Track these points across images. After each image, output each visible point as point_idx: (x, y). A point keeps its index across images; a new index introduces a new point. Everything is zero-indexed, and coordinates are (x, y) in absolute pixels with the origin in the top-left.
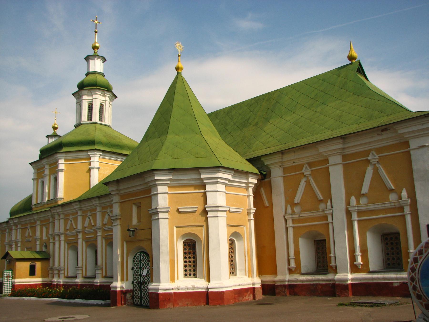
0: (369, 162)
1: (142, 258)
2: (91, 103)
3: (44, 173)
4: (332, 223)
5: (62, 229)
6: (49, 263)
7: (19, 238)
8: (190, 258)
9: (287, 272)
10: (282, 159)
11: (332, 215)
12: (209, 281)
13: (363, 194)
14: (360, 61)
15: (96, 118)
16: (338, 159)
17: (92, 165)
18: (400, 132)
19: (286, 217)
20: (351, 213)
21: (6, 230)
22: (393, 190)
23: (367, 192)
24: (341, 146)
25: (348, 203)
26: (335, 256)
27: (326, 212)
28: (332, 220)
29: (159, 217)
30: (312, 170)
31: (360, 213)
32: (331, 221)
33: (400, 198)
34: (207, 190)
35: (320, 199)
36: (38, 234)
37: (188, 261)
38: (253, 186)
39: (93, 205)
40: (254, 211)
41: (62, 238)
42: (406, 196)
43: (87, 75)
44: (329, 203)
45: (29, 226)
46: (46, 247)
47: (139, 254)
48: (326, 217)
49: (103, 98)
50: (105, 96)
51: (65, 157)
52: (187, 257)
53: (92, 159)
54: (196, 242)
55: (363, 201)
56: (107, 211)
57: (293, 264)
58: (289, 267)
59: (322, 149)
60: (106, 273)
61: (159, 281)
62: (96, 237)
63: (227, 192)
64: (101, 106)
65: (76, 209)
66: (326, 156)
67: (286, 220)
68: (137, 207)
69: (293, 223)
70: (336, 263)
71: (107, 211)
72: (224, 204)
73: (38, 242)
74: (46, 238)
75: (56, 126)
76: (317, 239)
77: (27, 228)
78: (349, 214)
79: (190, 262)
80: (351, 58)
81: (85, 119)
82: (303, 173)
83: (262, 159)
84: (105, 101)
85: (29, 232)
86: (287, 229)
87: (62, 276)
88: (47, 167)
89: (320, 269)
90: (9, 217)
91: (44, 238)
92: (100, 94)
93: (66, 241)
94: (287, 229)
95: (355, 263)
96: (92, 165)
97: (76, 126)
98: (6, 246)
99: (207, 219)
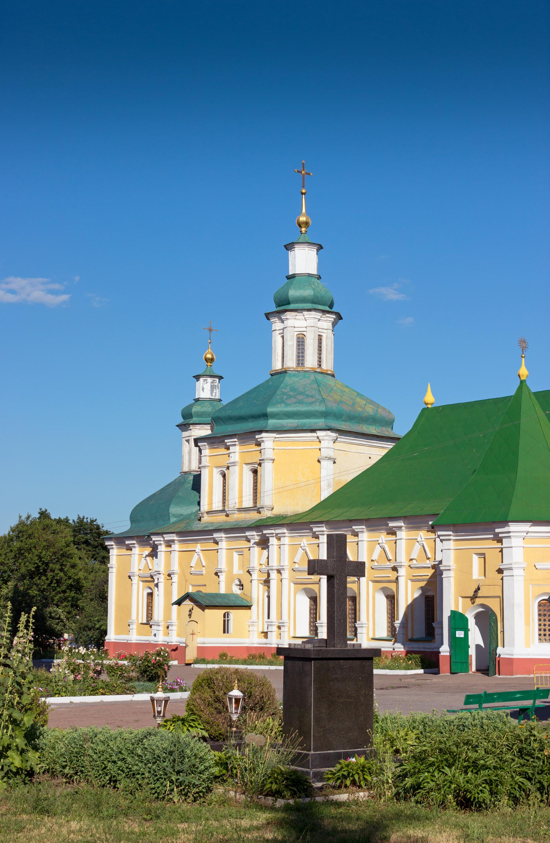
2: (304, 333)
8: (545, 620)
15: (310, 362)
29: (514, 574)
37: (542, 624)
41: (286, 574)
52: (542, 620)
53: (324, 444)
56: (378, 541)
60: (374, 633)
61: (512, 644)
71: (378, 541)
77: (195, 551)
91: (236, 570)
92: (319, 317)
96: (324, 453)
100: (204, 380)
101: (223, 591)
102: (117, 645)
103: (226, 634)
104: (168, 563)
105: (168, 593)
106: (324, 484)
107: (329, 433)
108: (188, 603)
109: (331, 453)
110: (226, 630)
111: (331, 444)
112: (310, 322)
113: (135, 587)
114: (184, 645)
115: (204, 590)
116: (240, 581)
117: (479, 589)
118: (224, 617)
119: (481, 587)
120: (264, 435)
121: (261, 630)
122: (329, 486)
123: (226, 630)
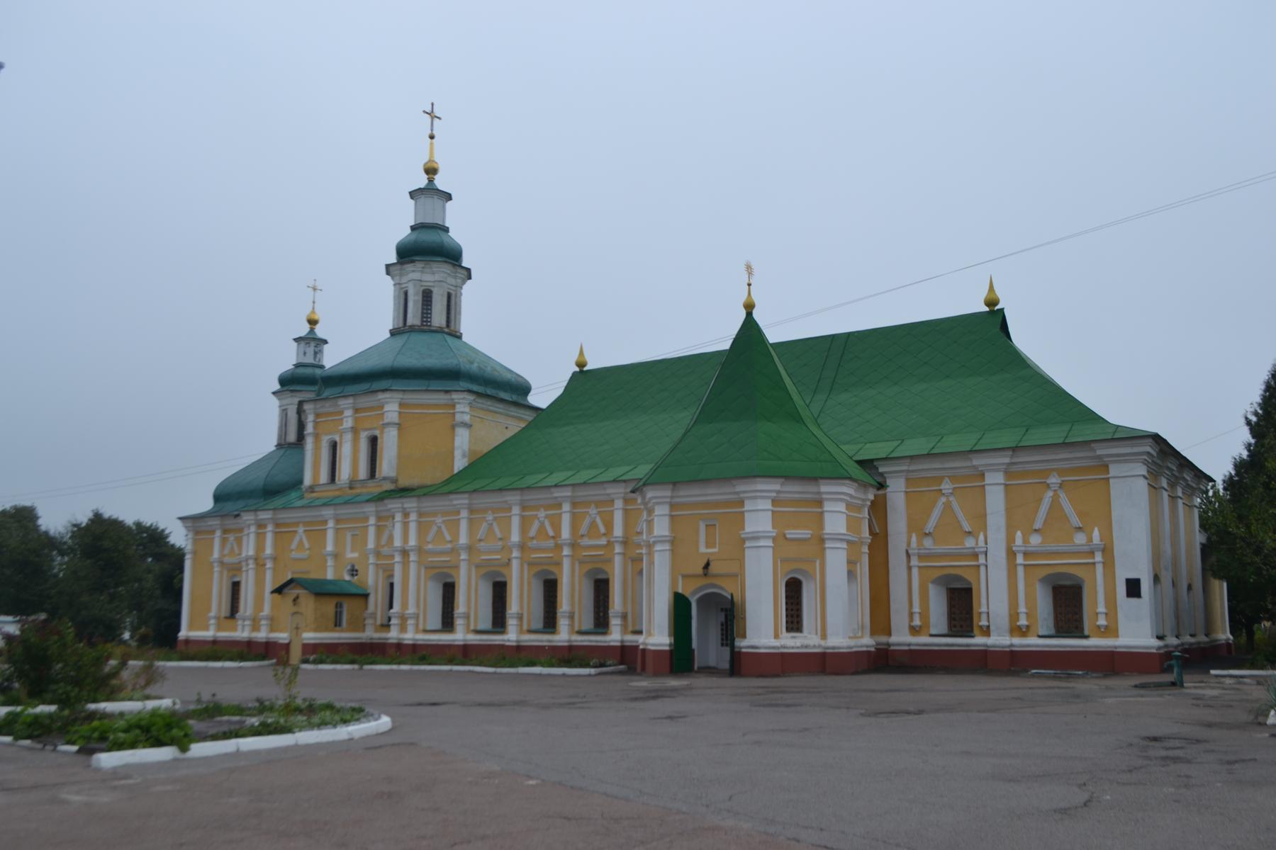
0: (1048, 486)
2: (432, 289)
3: (342, 425)
4: (987, 566)
5: (412, 542)
7: (269, 551)
9: (907, 630)
11: (986, 555)
12: (824, 636)
13: (1036, 530)
14: (1005, 311)
16: (999, 478)
17: (458, 418)
18: (1099, 452)
19: (910, 552)
20: (1015, 554)
21: (213, 532)
22: (1080, 528)
23: (1040, 527)
24: (1007, 460)
25: (1010, 539)
26: (988, 613)
28: (986, 561)
31: (1026, 554)
32: (984, 562)
33: (1090, 540)
34: (825, 509)
35: (967, 530)
38: (869, 503)
39: (506, 502)
40: (870, 541)
41: (413, 557)
42: (1099, 539)
43: (413, 228)
44: (981, 537)
45: (301, 529)
46: (353, 572)
49: (451, 280)
50: (455, 277)
51: (402, 399)
53: (459, 408)
55: (1035, 540)
58: (912, 624)
59: (978, 461)
60: (529, 624)
62: (507, 561)
63: (849, 514)
64: (449, 296)
65: (459, 506)
66: (982, 471)
67: (908, 555)
68: (707, 526)
70: (989, 621)
72: (844, 531)
73: (330, 562)
74: (355, 555)
75: (316, 317)
76: (949, 586)
78: (1011, 554)
80: (991, 302)
82: (941, 490)
83: (875, 463)
84: (456, 286)
86: (910, 568)
87: (410, 628)
88: (348, 413)
89: (953, 629)
90: (207, 504)
92: (449, 272)
93: (419, 563)
94: (910, 568)
95: (1018, 624)
96: (458, 418)
97: (394, 333)
98: (216, 564)
99: (824, 549)
100: (307, 343)
101: (330, 575)
102: (187, 642)
103: (338, 628)
104: (260, 547)
105: (260, 582)
106: (458, 454)
107: (465, 395)
108: (293, 592)
109: (467, 418)
111: (467, 409)
112: (437, 277)
113: (216, 575)
114: (286, 641)
115: (305, 576)
116: (353, 566)
117: (707, 566)
118: (336, 607)
119: (711, 564)
120: (387, 395)
121: (379, 622)
122: (464, 456)
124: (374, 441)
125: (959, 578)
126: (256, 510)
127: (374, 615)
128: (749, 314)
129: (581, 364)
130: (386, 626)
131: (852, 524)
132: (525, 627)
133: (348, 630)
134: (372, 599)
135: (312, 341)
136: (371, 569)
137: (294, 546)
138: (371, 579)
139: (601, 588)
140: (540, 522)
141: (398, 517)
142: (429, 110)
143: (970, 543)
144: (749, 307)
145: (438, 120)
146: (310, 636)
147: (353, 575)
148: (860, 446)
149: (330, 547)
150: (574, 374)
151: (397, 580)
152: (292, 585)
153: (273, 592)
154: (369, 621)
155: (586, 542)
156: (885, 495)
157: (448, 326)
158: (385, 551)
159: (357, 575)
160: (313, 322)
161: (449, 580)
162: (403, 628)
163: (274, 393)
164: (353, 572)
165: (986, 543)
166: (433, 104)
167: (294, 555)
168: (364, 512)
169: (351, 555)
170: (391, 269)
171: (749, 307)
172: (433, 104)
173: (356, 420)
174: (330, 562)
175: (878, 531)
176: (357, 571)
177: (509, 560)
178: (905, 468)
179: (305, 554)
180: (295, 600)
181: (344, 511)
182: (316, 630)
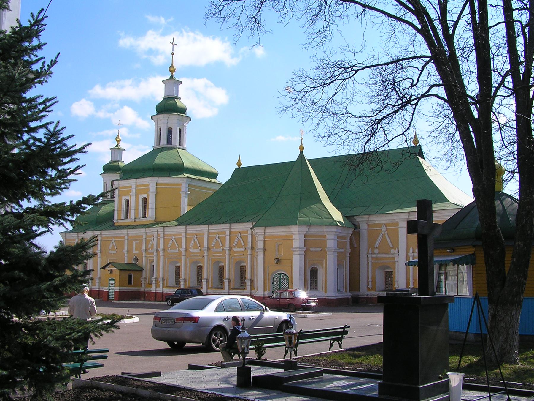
1: (281, 277)
4: (398, 262)
6: (142, 274)
8: (313, 278)
10: (368, 219)
11: (398, 257)
12: (326, 292)
19: (368, 255)
26: (398, 282)
27: (394, 255)
30: (386, 229)
36: (126, 248)
47: (279, 274)
48: (394, 258)
54: (317, 269)
57: (370, 285)
64: (180, 130)
69: (372, 260)
73: (126, 255)
74: (138, 252)
79: (313, 281)
81: (164, 141)
82: (381, 229)
83: (355, 217)
85: (113, 245)
86: (368, 263)
88: (134, 187)
94: (368, 263)
103: (130, 285)
110: (130, 283)
121: (148, 283)
123: (130, 283)
124: (145, 200)
125: (388, 267)
126: (93, 231)
127: (145, 279)
128: (302, 152)
129: (239, 164)
130: (151, 284)
131: (340, 245)
132: (210, 286)
133: (135, 286)
134: (144, 271)
135: (117, 150)
136: (144, 258)
137: (110, 247)
138: (143, 263)
139: (242, 270)
140: (216, 239)
141: (155, 235)
142: (172, 42)
143: (392, 251)
144: (302, 148)
145: (176, 45)
146: (117, 289)
147: (136, 261)
148: (351, 209)
149: (126, 248)
150: (236, 168)
151: (155, 264)
152: (109, 266)
153: (101, 269)
154: (143, 282)
155: (235, 249)
156: (359, 231)
157: (180, 145)
158: (150, 251)
159: (138, 261)
160: (118, 141)
161: (178, 265)
162: (157, 285)
163: (100, 175)
164: (137, 260)
165: (398, 253)
166: (173, 38)
167: (111, 252)
168: (141, 233)
169: (134, 252)
170: (153, 118)
171: (302, 148)
172: (173, 38)
173: (136, 190)
174: (126, 255)
175: (356, 246)
176: (138, 259)
177: (203, 256)
178: (367, 220)
179: (115, 252)
180: (111, 271)
181: (132, 232)
182: (120, 286)
